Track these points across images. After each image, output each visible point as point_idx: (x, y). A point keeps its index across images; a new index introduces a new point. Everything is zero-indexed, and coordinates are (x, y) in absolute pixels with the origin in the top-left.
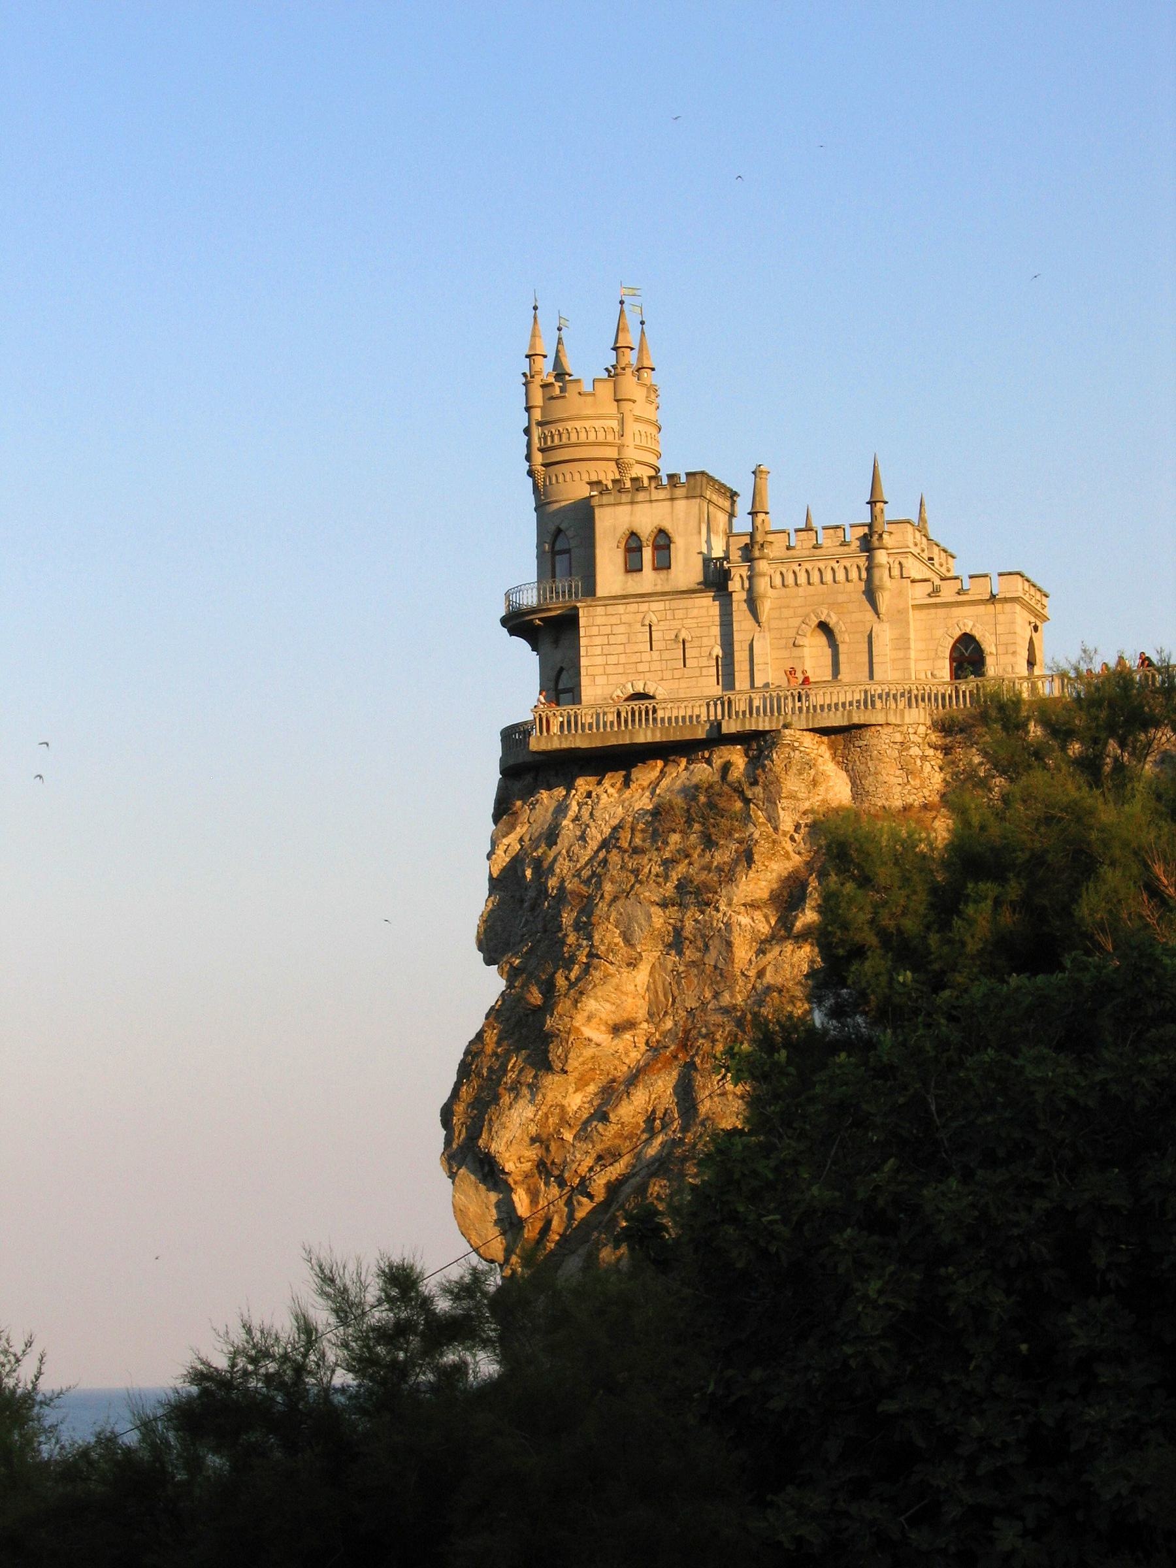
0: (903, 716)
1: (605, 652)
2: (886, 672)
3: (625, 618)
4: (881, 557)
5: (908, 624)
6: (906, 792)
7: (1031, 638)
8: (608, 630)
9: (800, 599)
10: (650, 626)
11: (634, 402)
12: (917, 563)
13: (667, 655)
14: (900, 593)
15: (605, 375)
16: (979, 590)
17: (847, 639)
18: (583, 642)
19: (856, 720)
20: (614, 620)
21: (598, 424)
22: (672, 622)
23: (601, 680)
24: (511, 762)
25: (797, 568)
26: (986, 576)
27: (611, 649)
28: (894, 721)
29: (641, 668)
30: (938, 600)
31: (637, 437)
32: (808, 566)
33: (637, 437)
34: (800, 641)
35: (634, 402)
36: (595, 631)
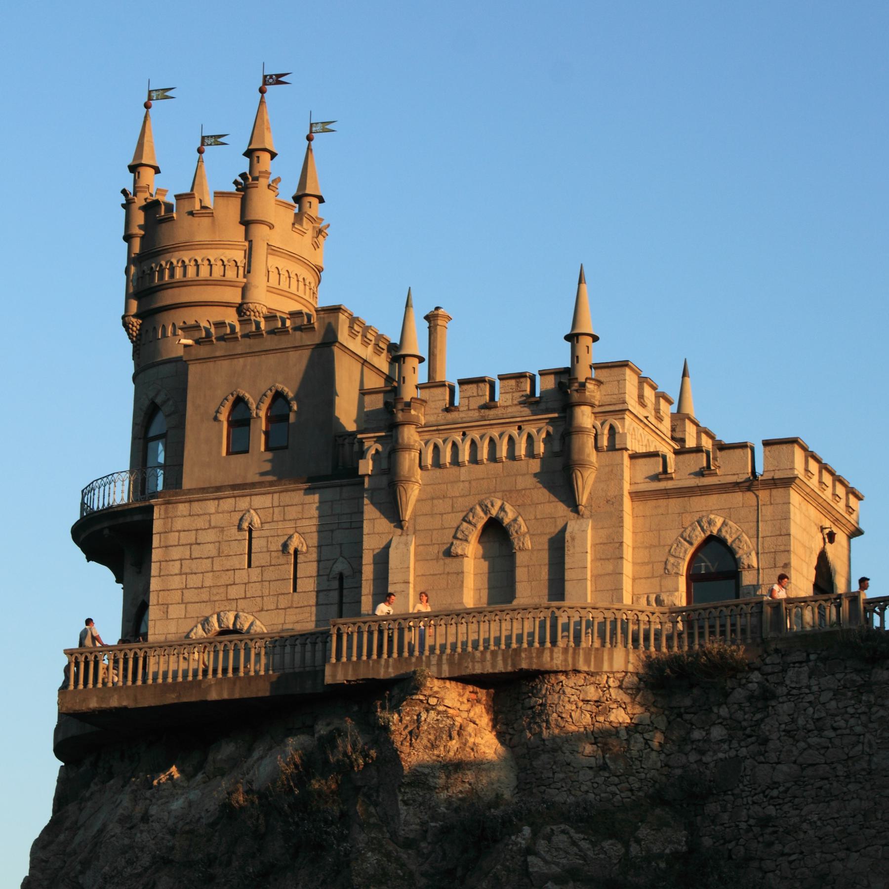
0: (599, 661)
1: (184, 571)
2: (585, 590)
3: (216, 520)
4: (585, 417)
5: (621, 519)
6: (600, 780)
7: (823, 557)
8: (191, 537)
9: (461, 485)
10: (250, 531)
11: (271, 227)
12: (640, 430)
13: (270, 574)
14: (613, 474)
15: (233, 188)
16: (730, 468)
17: (528, 544)
18: (156, 555)
19: (524, 665)
20: (200, 523)
21: (213, 254)
22: (280, 525)
23: (176, 611)
24: (60, 738)
25: (458, 438)
26: (743, 446)
27: (194, 565)
28: (586, 669)
29: (234, 592)
30: (669, 485)
31: (274, 276)
32: (475, 434)
33: (274, 276)
34: (458, 548)
35: (271, 227)
36: (173, 538)
